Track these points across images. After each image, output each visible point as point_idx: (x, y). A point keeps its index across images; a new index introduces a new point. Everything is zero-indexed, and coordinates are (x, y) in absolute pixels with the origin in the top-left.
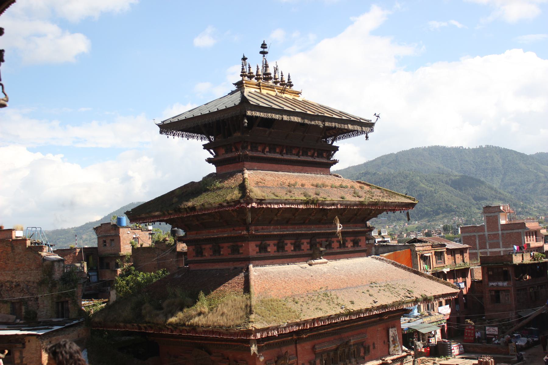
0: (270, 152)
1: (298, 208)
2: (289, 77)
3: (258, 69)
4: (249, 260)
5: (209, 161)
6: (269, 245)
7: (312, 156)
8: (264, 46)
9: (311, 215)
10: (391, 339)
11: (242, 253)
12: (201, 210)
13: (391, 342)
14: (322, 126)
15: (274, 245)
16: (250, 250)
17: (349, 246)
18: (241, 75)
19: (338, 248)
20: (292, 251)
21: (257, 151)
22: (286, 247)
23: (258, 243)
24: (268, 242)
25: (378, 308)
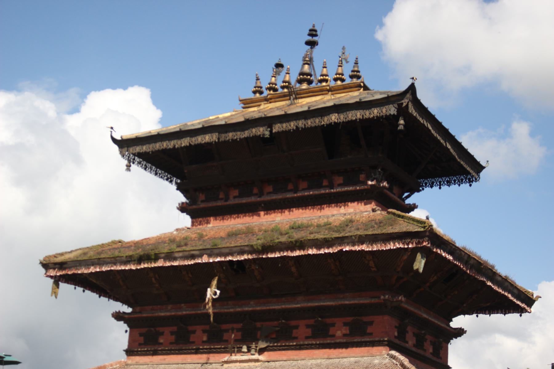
0: (240, 196)
2: (356, 63)
6: (162, 334)
8: (313, 33)
14: (267, 134)
15: (172, 333)
17: (339, 333)
18: (255, 92)
19: (307, 338)
20: (204, 342)
21: (217, 199)
24: (161, 329)
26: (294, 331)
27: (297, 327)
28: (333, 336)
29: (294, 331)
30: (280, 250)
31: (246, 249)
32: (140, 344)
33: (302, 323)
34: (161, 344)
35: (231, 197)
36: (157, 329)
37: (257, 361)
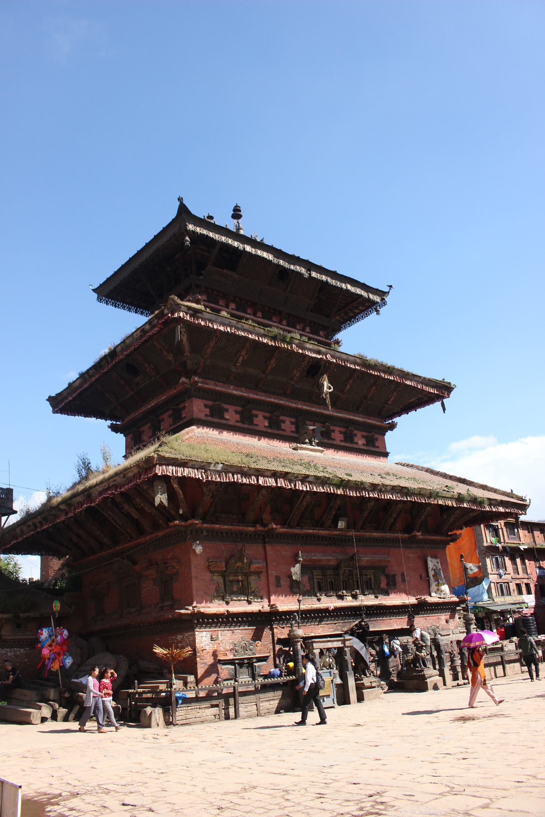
6: (227, 410)
9: (292, 379)
10: (431, 573)
11: (185, 417)
12: (123, 350)
13: (432, 578)
14: (306, 275)
15: (236, 412)
16: (195, 409)
17: (360, 442)
19: (341, 441)
20: (265, 427)
21: (218, 305)
23: (210, 403)
24: (225, 406)
25: (394, 489)
26: (332, 434)
27: (334, 431)
28: (357, 443)
29: (332, 434)
30: (379, 371)
31: (358, 360)
33: (337, 429)
34: (228, 420)
35: (230, 308)
36: (223, 405)
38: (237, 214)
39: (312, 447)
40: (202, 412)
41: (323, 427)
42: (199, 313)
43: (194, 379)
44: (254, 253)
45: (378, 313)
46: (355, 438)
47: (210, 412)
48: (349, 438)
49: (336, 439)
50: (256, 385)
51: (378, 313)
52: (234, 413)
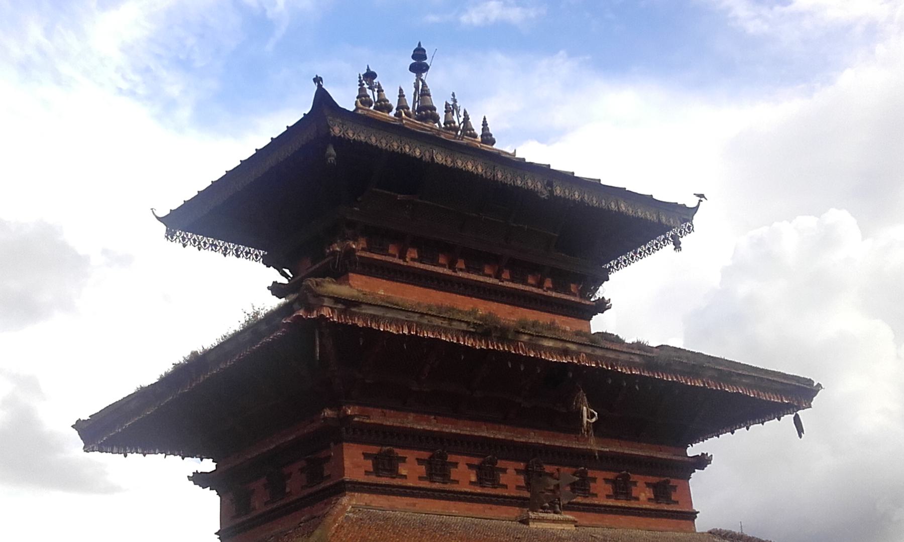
1: (458, 345)
2: (485, 124)
3: (401, 95)
4: (341, 488)
5: (276, 289)
6: (403, 459)
7: (540, 285)
8: (419, 54)
11: (329, 476)
14: (545, 195)
15: (420, 461)
16: (347, 463)
17: (643, 497)
19: (608, 497)
20: (471, 483)
22: (453, 470)
26: (592, 485)
27: (594, 480)
28: (637, 499)
29: (592, 485)
30: (675, 373)
31: (637, 359)
32: (367, 473)
33: (600, 475)
34: (405, 477)
36: (396, 450)
37: (573, 522)
38: (419, 66)
39: (556, 516)
40: (359, 467)
41: (574, 475)
42: (355, 306)
43: (345, 412)
44: (449, 163)
45: (677, 246)
46: (633, 488)
47: (373, 464)
48: (622, 489)
49: (599, 495)
50: (454, 408)
51: (677, 246)
52: (416, 462)
